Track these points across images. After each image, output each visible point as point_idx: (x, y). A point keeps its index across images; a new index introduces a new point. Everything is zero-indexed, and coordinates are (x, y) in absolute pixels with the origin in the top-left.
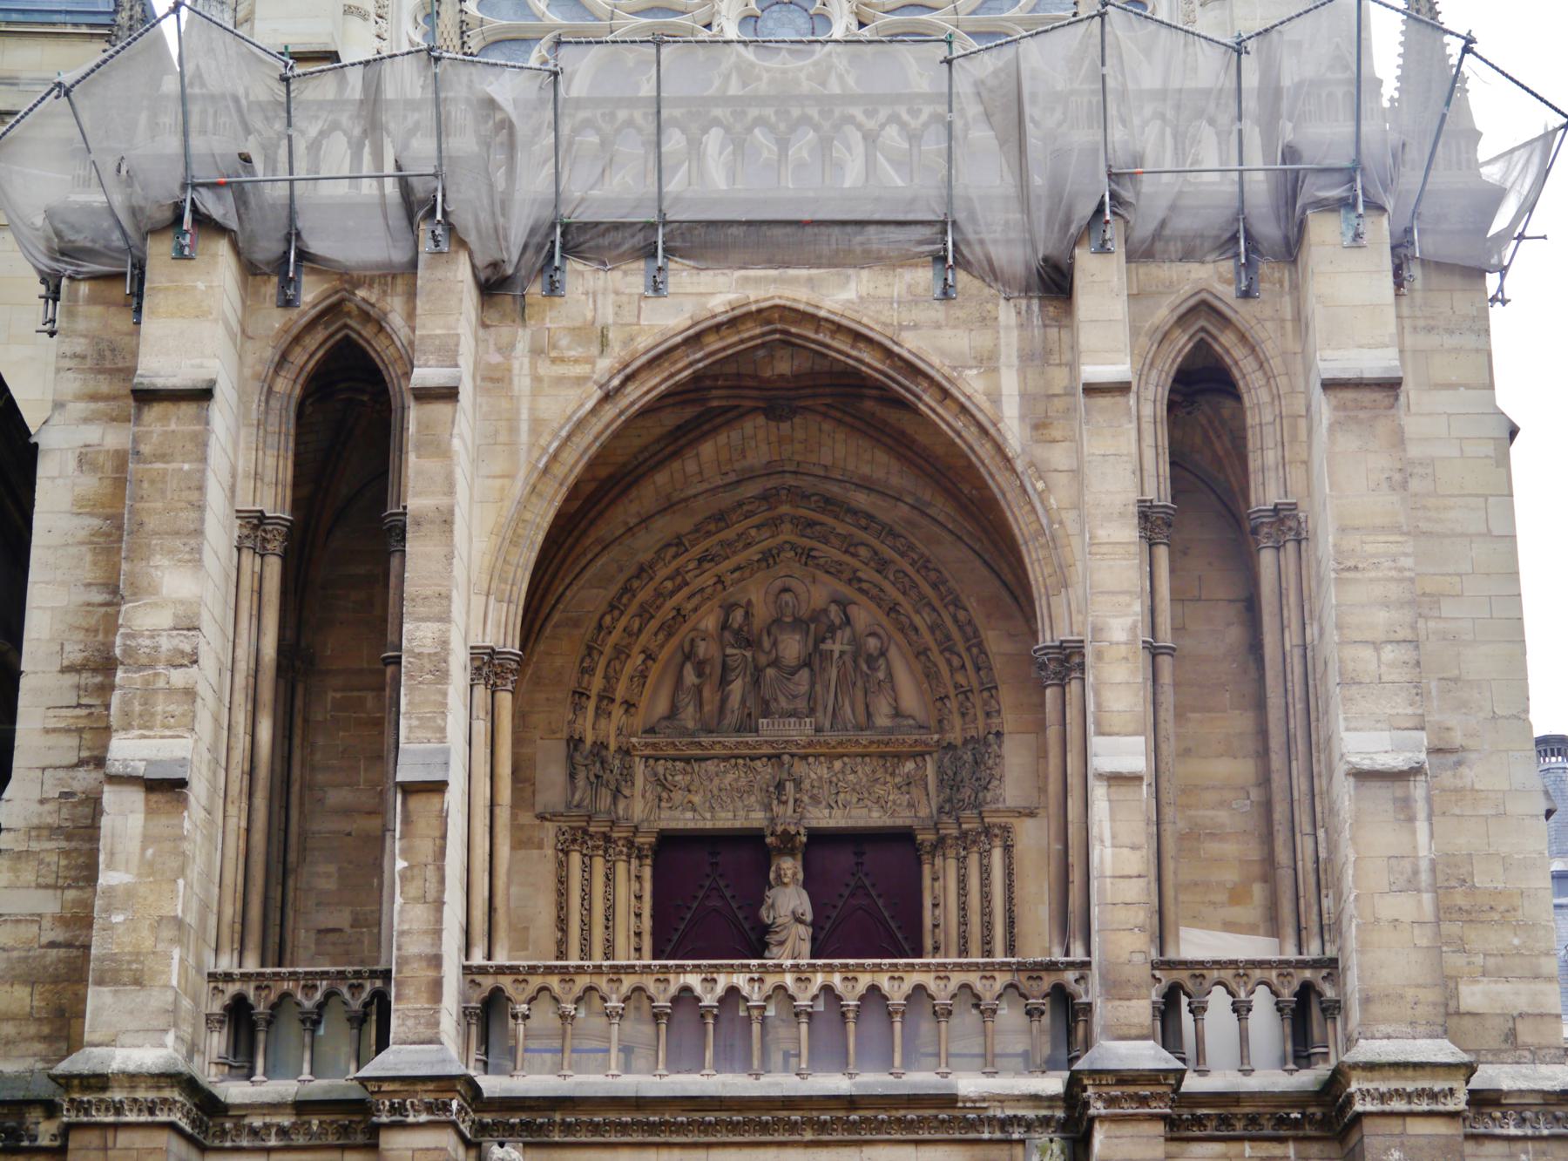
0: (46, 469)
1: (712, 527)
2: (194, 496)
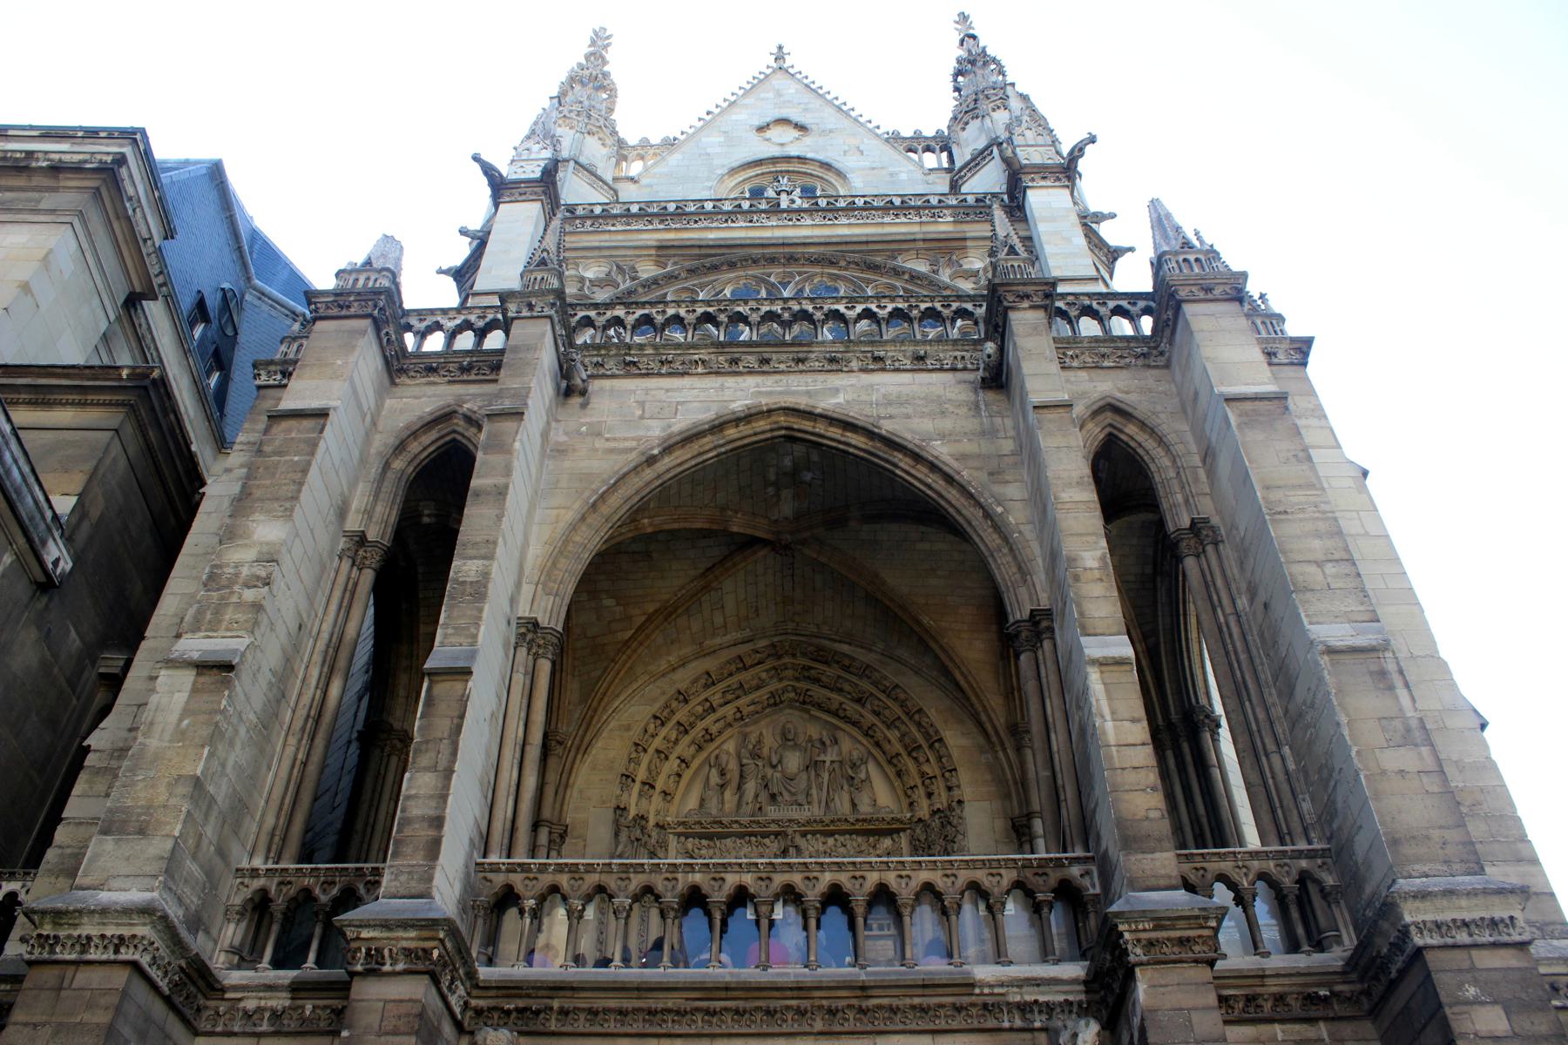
0: (205, 507)
1: (733, 668)
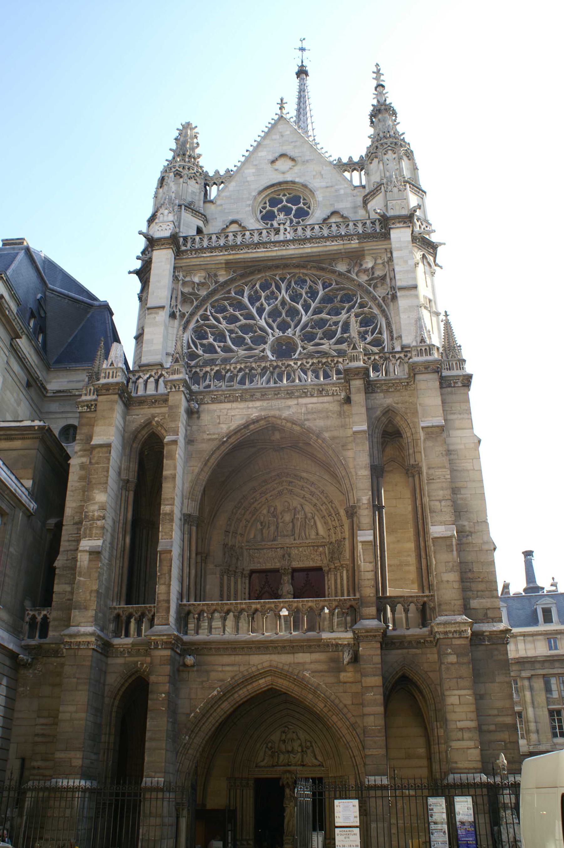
0: (71, 470)
1: (264, 484)
2: (105, 473)
